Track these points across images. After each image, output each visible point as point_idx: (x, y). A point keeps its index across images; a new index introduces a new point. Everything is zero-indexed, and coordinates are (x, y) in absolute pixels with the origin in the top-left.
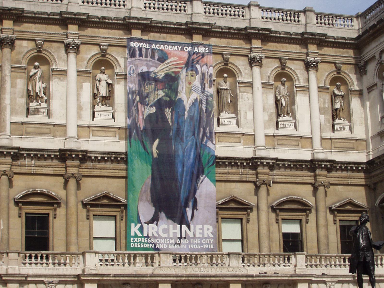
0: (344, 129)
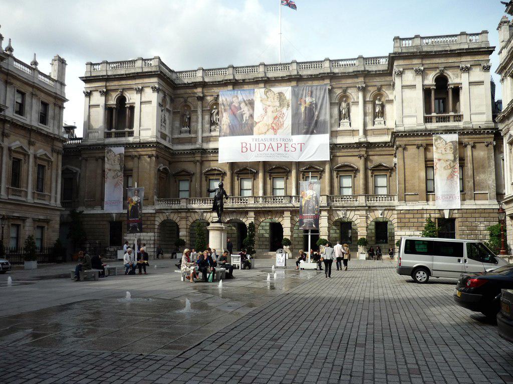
0: (381, 123)
